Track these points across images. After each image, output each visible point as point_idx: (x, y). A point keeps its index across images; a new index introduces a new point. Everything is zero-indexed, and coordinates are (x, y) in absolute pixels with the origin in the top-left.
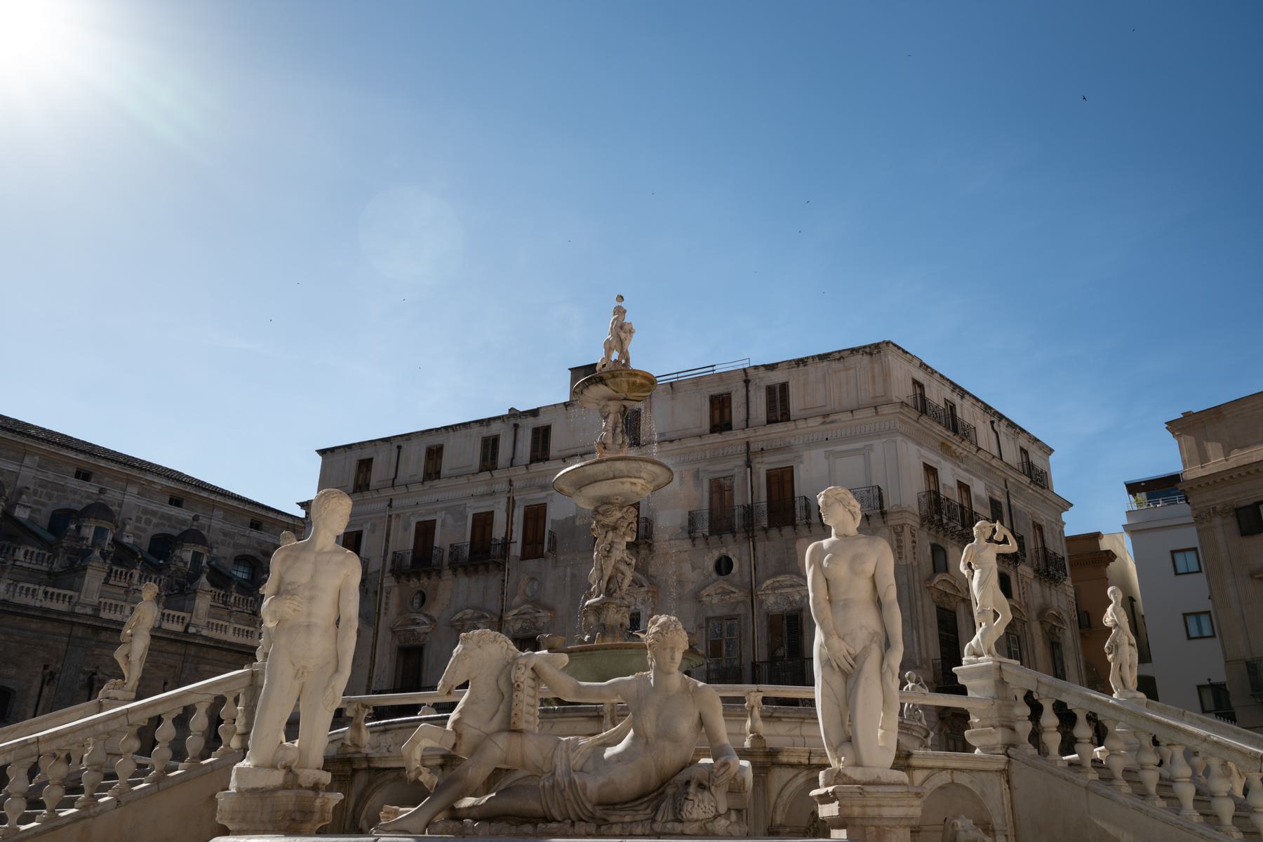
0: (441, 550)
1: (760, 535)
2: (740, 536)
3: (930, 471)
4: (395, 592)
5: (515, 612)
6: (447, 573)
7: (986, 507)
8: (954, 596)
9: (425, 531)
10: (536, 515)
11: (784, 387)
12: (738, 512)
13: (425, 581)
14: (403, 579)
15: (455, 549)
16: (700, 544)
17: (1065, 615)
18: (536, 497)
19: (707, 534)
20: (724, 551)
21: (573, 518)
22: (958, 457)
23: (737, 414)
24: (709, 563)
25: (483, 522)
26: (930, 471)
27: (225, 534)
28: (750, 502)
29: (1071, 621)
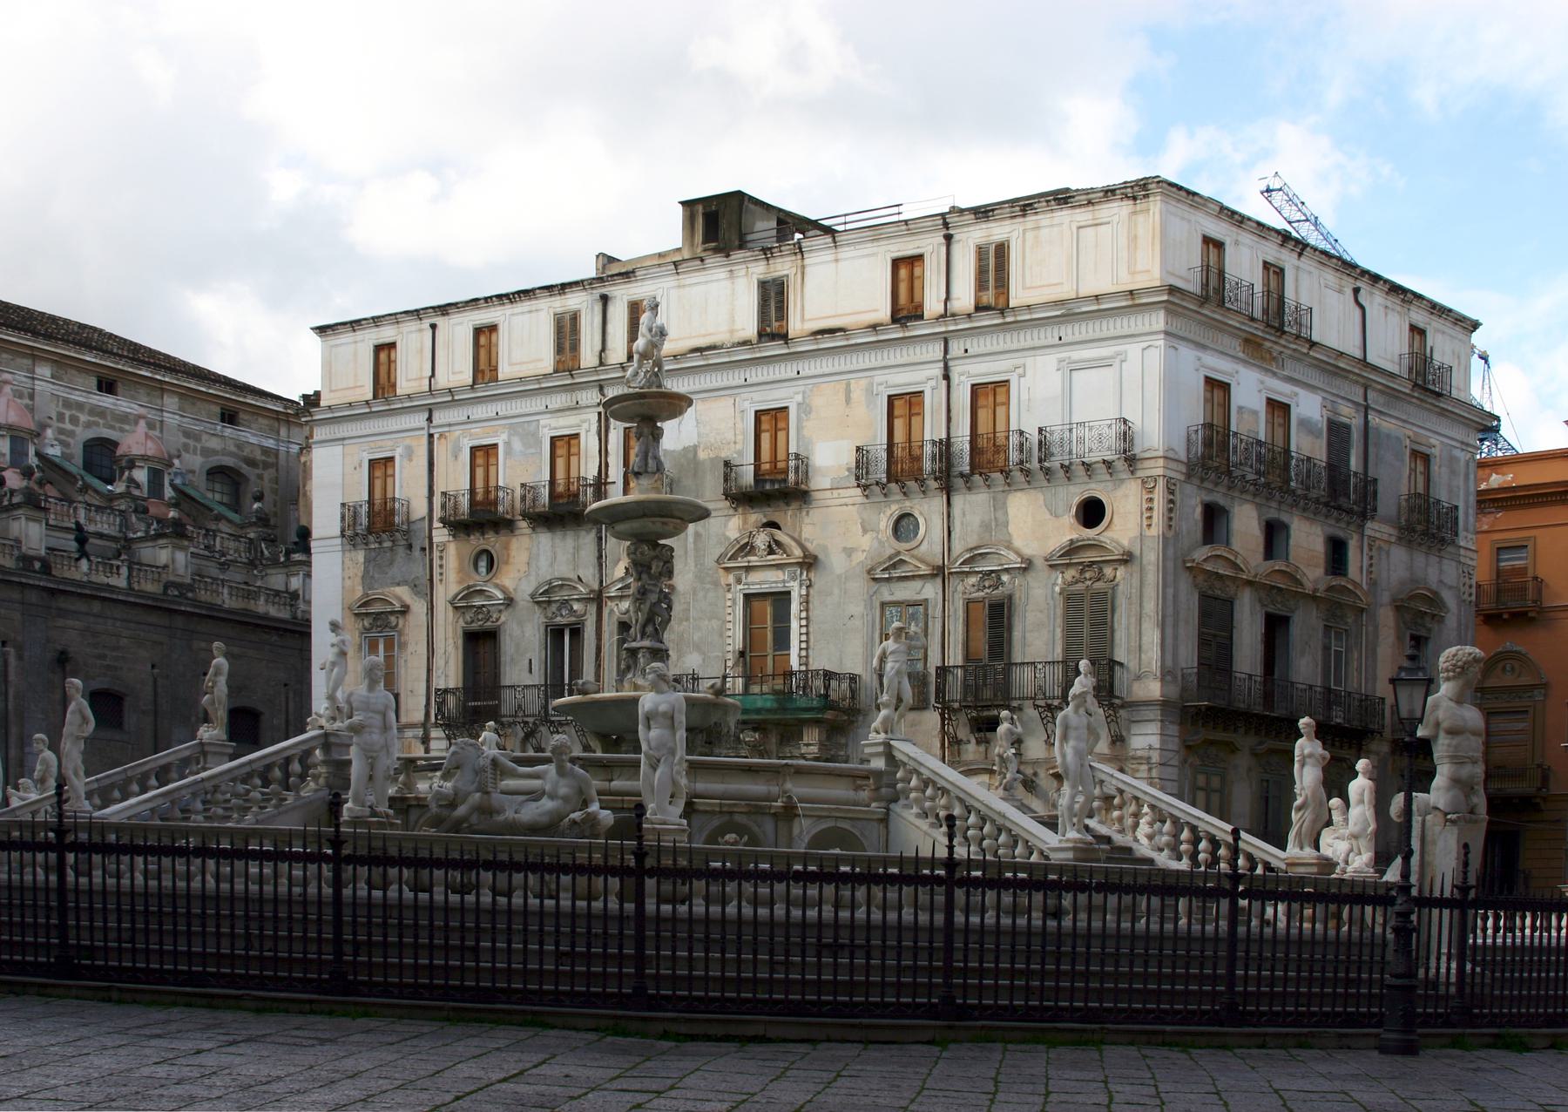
1: (959, 482)
2: (933, 484)
3: (1217, 388)
7: (1317, 435)
8: (1234, 579)
12: (928, 449)
17: (1448, 598)
19: (885, 480)
20: (907, 506)
21: (695, 448)
22: (1274, 359)
24: (885, 522)
26: (1217, 388)
27: (187, 434)
28: (944, 436)
29: (1461, 602)
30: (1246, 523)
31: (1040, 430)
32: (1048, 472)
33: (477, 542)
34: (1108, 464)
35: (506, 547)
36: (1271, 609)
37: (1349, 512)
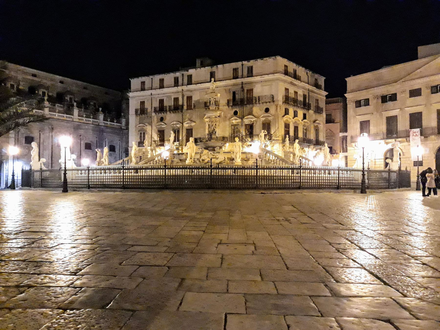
0: (166, 107)
3: (287, 90)
4: (155, 117)
5: (186, 123)
6: (168, 113)
7: (302, 96)
9: (161, 101)
10: (189, 98)
11: (252, 67)
13: (163, 114)
14: (157, 114)
15: (170, 107)
16: (230, 107)
18: (189, 94)
20: (236, 109)
21: (199, 100)
23: (240, 74)
25: (176, 100)
26: (287, 90)
30: (291, 111)
31: (259, 97)
32: (259, 103)
33: (161, 115)
34: (270, 102)
35: (166, 116)
36: (295, 125)
37: (307, 109)
